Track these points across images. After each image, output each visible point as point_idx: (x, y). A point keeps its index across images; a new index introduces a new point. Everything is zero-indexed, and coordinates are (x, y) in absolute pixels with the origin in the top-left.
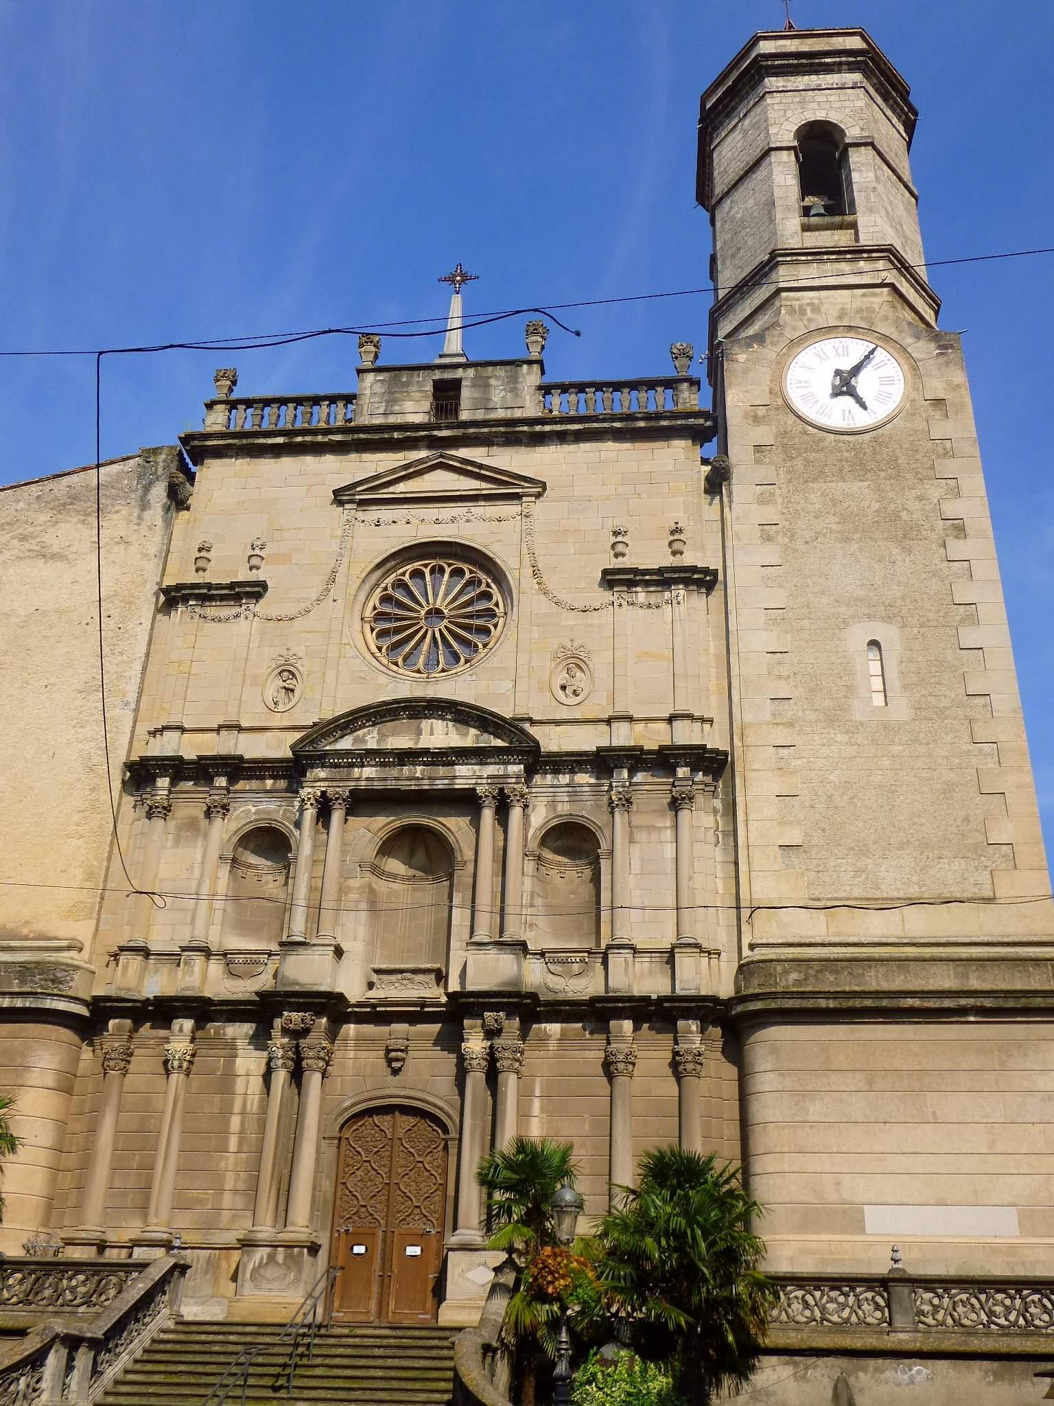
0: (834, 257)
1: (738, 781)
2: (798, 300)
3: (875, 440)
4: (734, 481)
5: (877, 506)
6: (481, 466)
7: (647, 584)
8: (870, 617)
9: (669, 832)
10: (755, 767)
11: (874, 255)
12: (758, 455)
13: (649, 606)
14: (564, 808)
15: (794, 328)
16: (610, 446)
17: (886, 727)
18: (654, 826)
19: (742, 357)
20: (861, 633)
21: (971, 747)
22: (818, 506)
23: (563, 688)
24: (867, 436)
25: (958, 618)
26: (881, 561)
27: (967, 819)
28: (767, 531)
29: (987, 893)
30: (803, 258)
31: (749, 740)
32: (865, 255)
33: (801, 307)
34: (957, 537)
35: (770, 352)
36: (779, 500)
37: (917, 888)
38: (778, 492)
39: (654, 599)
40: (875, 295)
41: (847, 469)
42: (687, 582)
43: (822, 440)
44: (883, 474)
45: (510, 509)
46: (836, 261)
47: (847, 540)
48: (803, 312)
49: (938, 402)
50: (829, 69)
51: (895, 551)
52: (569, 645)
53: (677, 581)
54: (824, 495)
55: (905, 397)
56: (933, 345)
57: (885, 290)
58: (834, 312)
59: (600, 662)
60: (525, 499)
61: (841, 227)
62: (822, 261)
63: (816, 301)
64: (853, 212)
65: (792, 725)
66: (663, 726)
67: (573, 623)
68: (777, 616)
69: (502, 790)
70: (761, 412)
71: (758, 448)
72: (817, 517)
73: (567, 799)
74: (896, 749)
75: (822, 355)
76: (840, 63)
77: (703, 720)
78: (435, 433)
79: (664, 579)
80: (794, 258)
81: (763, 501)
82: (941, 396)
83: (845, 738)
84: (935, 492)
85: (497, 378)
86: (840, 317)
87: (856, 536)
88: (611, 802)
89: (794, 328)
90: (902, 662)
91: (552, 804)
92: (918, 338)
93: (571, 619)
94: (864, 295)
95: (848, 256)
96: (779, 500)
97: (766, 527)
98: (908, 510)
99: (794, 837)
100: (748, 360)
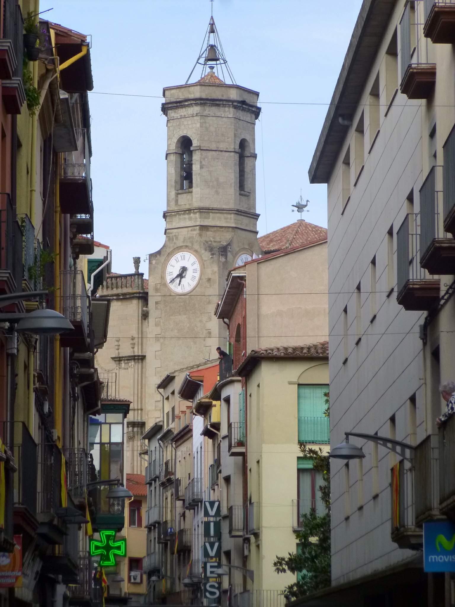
0: (183, 212)
2: (171, 233)
4: (150, 317)
5: (188, 325)
11: (195, 211)
13: (125, 369)
15: (170, 248)
28: (157, 338)
32: (192, 211)
33: (172, 236)
36: (162, 324)
40: (195, 230)
41: (181, 310)
42: (134, 359)
44: (191, 312)
46: (184, 214)
49: (209, 280)
51: (192, 343)
55: (200, 279)
56: (210, 253)
57: (198, 227)
62: (180, 215)
63: (177, 234)
71: (157, 303)
72: (172, 331)
75: (177, 260)
76: (191, 104)
77: (138, 410)
80: (171, 213)
81: (157, 325)
86: (184, 242)
92: (206, 250)
94: (191, 230)
98: (196, 326)
100: (156, 263)
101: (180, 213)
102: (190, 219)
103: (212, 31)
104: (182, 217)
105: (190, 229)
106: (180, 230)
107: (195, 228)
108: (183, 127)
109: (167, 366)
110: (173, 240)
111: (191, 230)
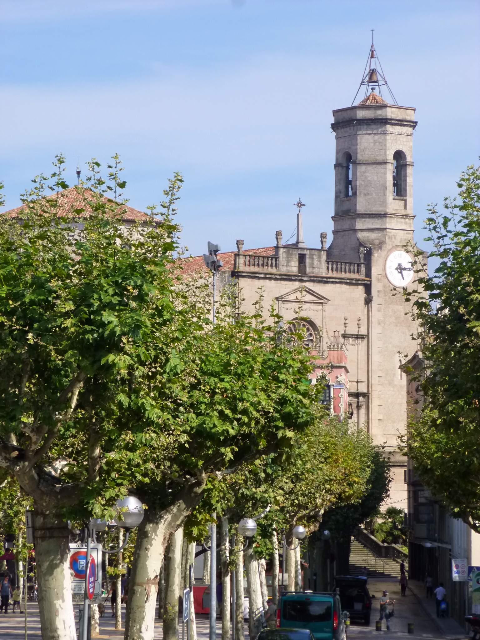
2: (390, 233)
6: (314, 292)
7: (352, 337)
13: (352, 345)
16: (344, 285)
39: (353, 343)
40: (409, 234)
45: (320, 307)
47: (397, 326)
51: (407, 331)
53: (359, 338)
58: (398, 238)
61: (402, 200)
62: (398, 218)
64: (406, 196)
65: (382, 385)
78: (303, 278)
79: (357, 337)
81: (379, 310)
83: (392, 389)
85: (315, 255)
86: (400, 242)
94: (407, 233)
96: (382, 310)
99: (381, 417)
102: (406, 223)
103: (372, 57)
104: (399, 220)
105: (406, 232)
108: (399, 142)
110: (392, 239)
111: (407, 233)
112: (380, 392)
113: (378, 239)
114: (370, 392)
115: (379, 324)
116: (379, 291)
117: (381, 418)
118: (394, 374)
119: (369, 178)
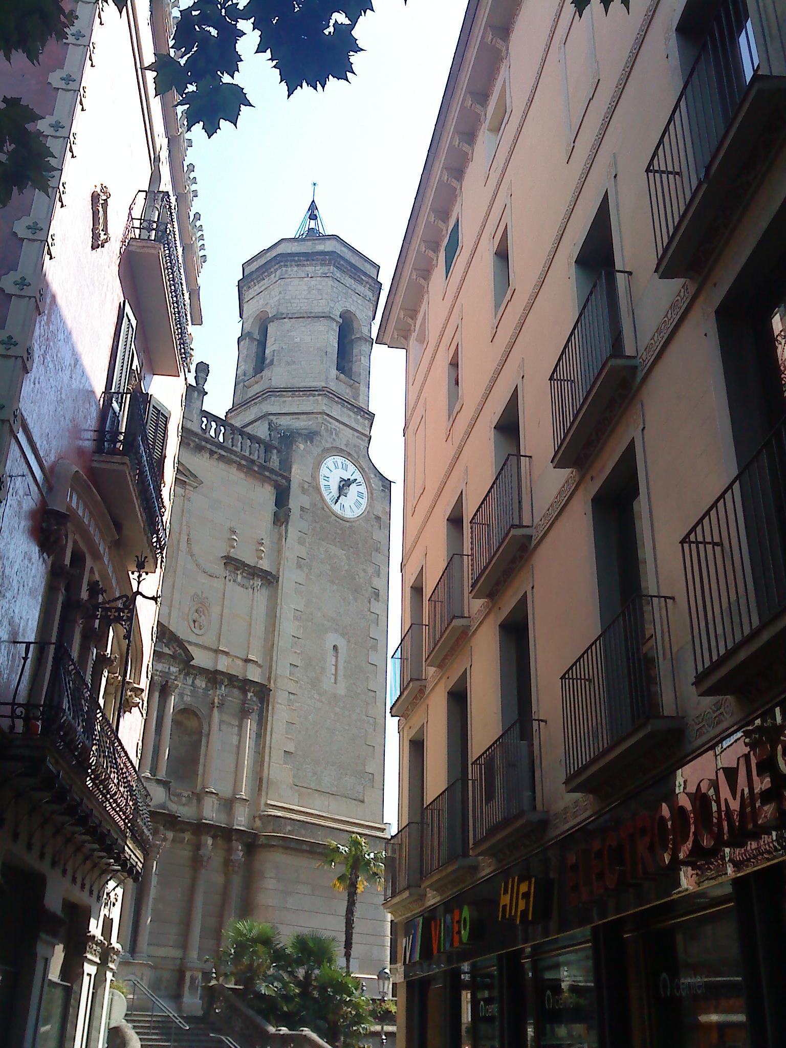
0: (349, 406)
1: (270, 707)
3: (350, 527)
5: (347, 567)
8: (336, 631)
9: (237, 728)
10: (280, 702)
11: (366, 416)
12: (302, 512)
13: (243, 586)
14: (187, 699)
17: (335, 696)
18: (230, 723)
19: (302, 446)
20: (332, 639)
21: (365, 718)
22: (323, 556)
23: (194, 621)
24: (348, 524)
25: (370, 645)
26: (344, 599)
27: (358, 757)
29: (361, 798)
30: (337, 399)
31: (279, 685)
34: (375, 599)
35: (316, 451)
37: (336, 789)
38: (307, 540)
39: (245, 582)
43: (330, 517)
44: (352, 550)
46: (349, 409)
47: (333, 583)
48: (332, 434)
50: (360, 282)
51: (351, 597)
52: (200, 594)
54: (326, 551)
56: (380, 483)
59: (215, 611)
60: (187, 487)
66: (240, 663)
67: (204, 581)
68: (298, 615)
69: (167, 681)
70: (306, 486)
73: (189, 694)
74: (338, 710)
76: (367, 283)
79: (254, 572)
80: (333, 396)
81: (301, 542)
82: (380, 516)
84: (370, 570)
87: (337, 582)
88: (213, 703)
89: (327, 441)
90: (345, 662)
91: (181, 695)
93: (203, 579)
95: (355, 410)
96: (307, 545)
97: (300, 559)
99: (291, 748)
101: (346, 404)
102: (357, 421)
106: (342, 426)
107: (364, 438)
109: (312, 615)
112: (292, 696)
113: (306, 429)
114: (281, 573)
115: (299, 567)
116: (302, 509)
117: (292, 750)
118: (323, 669)
119: (298, 340)
